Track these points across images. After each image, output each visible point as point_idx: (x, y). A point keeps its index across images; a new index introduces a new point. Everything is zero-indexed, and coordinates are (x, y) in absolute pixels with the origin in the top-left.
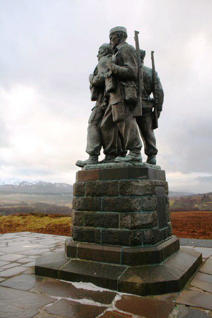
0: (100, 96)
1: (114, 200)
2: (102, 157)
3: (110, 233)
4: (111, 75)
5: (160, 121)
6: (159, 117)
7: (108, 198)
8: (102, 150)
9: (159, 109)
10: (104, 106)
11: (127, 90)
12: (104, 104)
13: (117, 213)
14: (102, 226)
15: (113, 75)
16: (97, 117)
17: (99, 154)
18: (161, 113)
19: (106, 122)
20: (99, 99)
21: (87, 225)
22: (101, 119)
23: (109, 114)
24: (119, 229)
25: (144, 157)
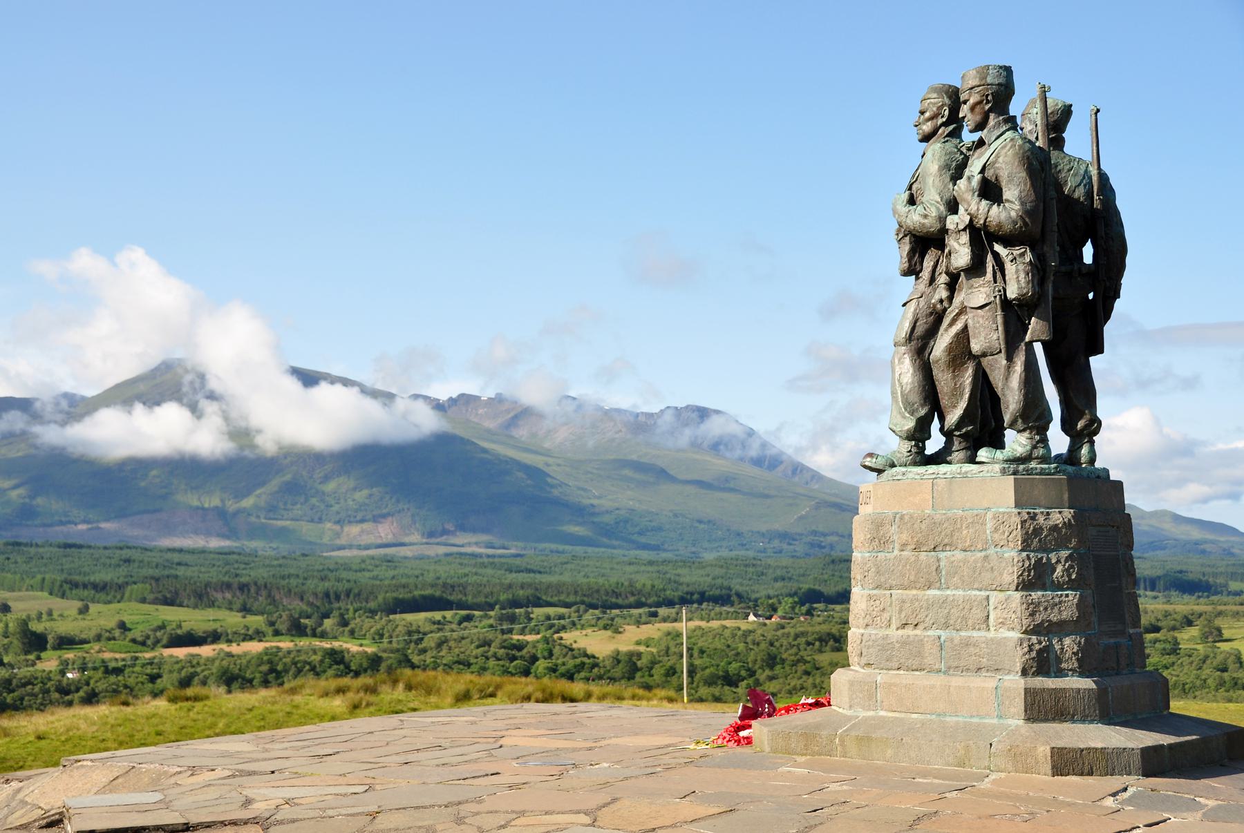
0: (928, 263)
1: (976, 561)
2: (935, 443)
3: (967, 643)
4: (964, 230)
5: (1109, 330)
6: (1107, 317)
7: (959, 555)
8: (936, 424)
9: (1111, 293)
10: (941, 301)
11: (1010, 268)
12: (943, 293)
13: (984, 593)
14: (946, 626)
15: (971, 227)
16: (920, 330)
17: (929, 437)
18: (1118, 305)
19: (950, 349)
20: (926, 274)
21: (904, 625)
22: (932, 332)
23: (959, 326)
24: (992, 634)
25: (1059, 441)
